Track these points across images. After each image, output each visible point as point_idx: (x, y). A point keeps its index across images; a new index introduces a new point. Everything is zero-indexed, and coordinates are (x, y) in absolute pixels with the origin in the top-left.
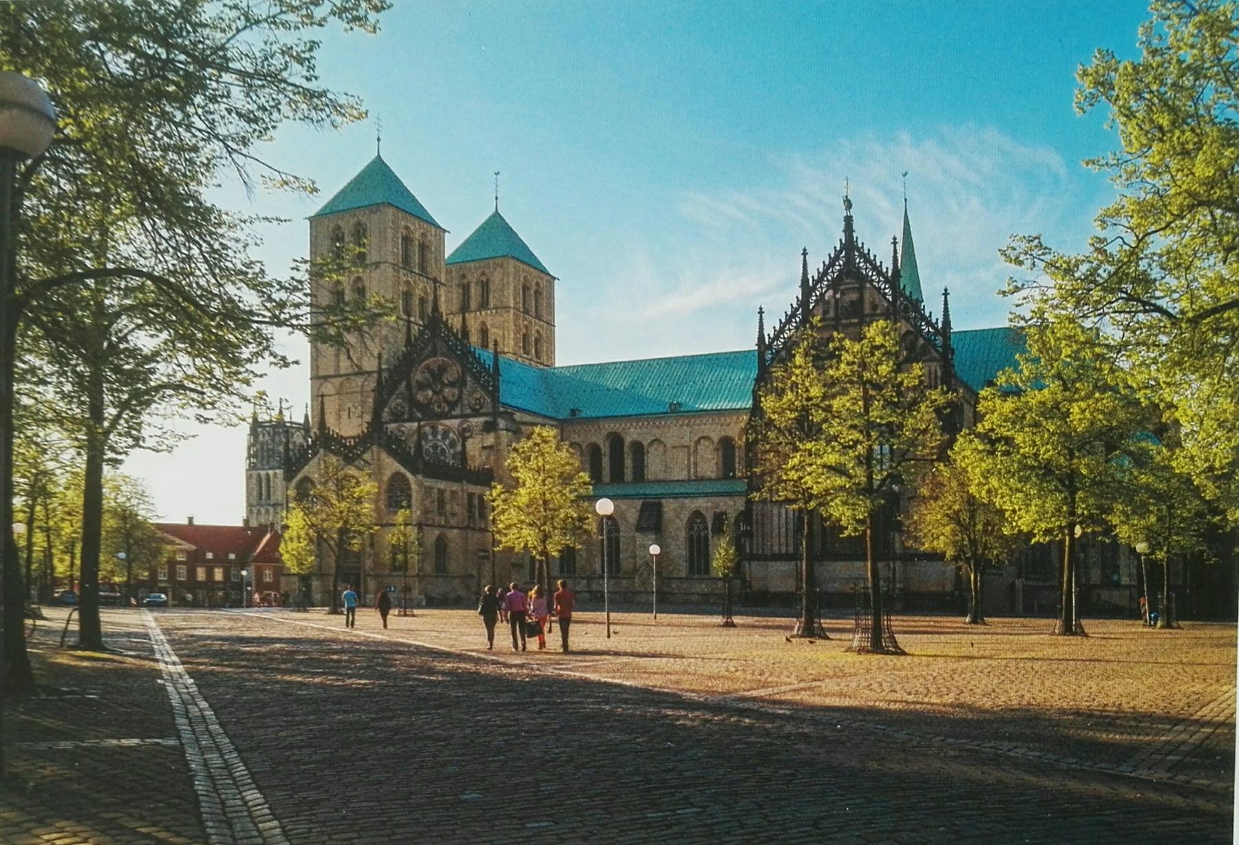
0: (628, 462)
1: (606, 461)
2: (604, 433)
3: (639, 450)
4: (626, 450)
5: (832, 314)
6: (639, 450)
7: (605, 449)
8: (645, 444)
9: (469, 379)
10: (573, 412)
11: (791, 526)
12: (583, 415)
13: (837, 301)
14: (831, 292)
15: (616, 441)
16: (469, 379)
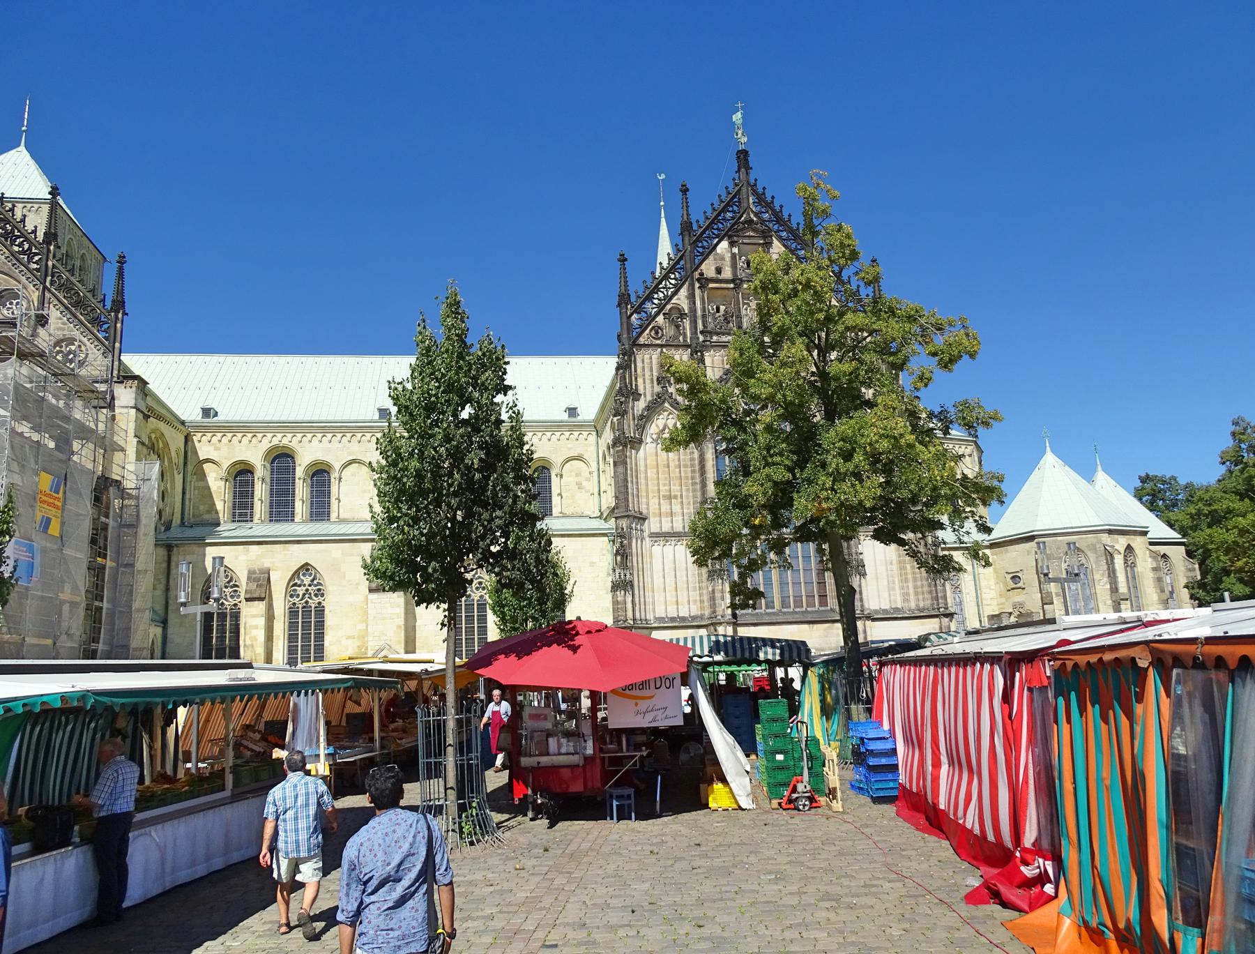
0: (302, 491)
1: (261, 491)
2: (265, 445)
3: (320, 475)
4: (299, 472)
5: (727, 273)
6: (320, 475)
7: (260, 471)
8: (337, 466)
9: (54, 314)
10: (207, 412)
11: (681, 574)
12: (221, 417)
13: (733, 255)
14: (724, 244)
15: (282, 459)
16: (54, 314)
